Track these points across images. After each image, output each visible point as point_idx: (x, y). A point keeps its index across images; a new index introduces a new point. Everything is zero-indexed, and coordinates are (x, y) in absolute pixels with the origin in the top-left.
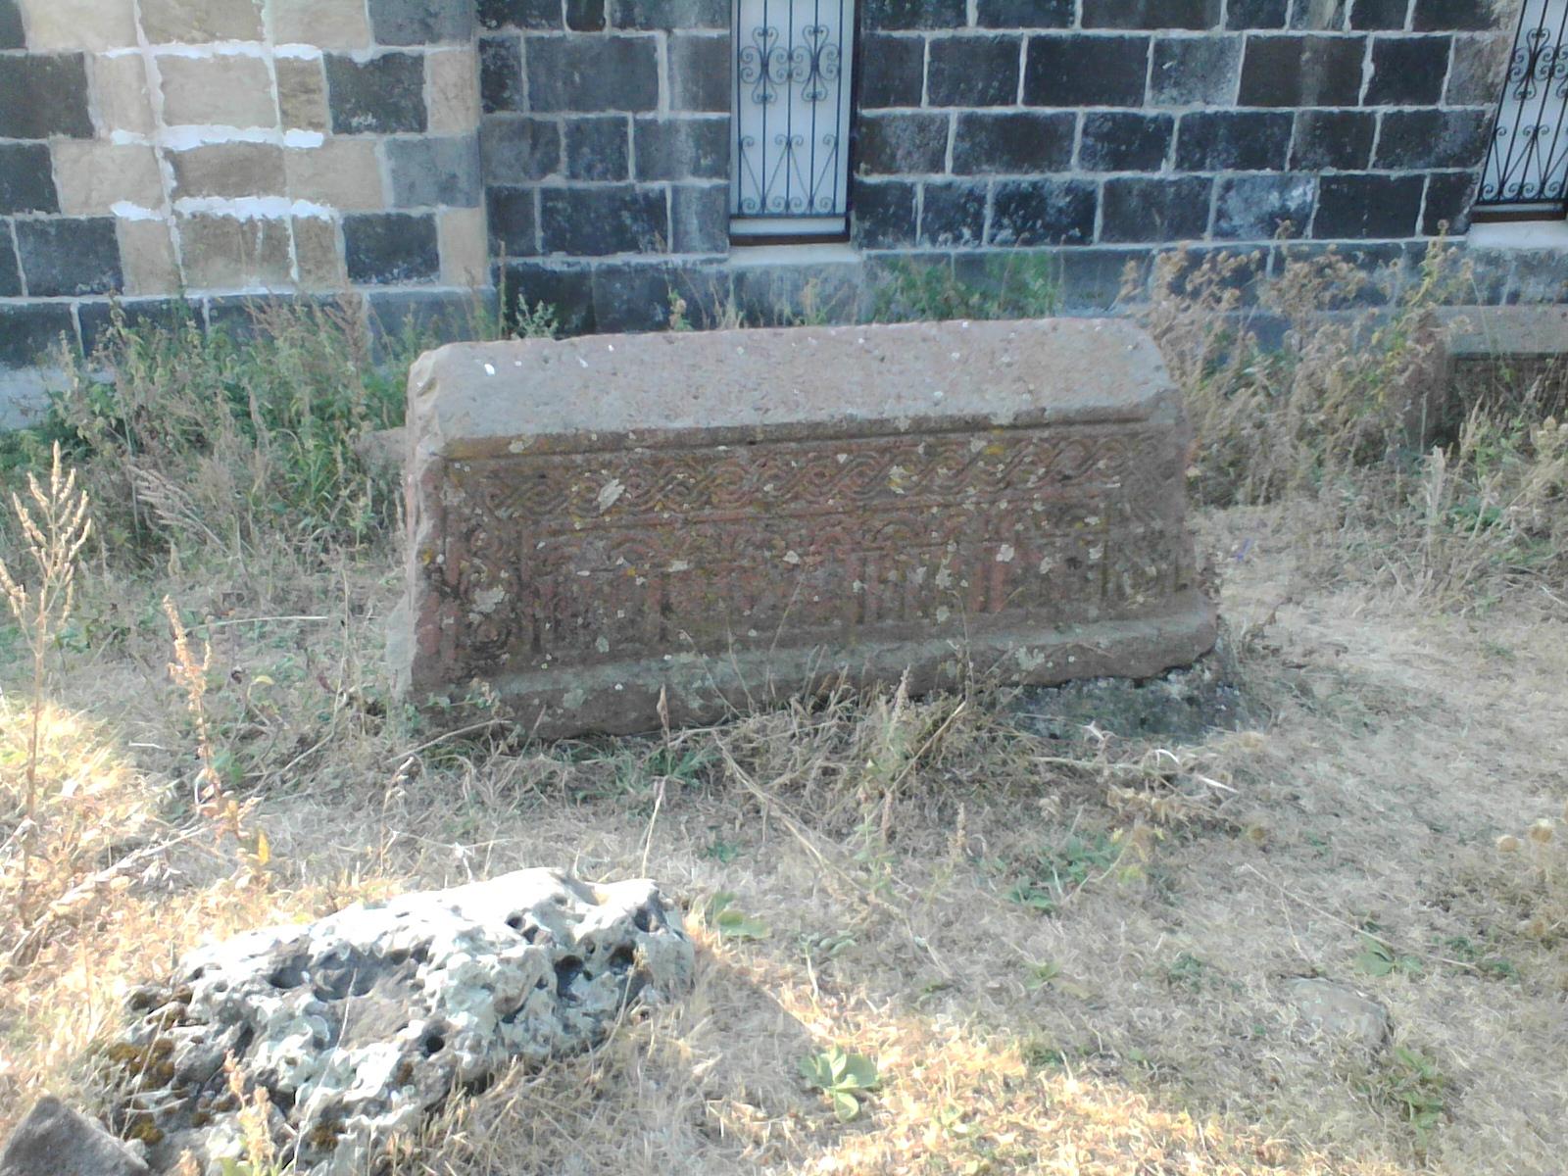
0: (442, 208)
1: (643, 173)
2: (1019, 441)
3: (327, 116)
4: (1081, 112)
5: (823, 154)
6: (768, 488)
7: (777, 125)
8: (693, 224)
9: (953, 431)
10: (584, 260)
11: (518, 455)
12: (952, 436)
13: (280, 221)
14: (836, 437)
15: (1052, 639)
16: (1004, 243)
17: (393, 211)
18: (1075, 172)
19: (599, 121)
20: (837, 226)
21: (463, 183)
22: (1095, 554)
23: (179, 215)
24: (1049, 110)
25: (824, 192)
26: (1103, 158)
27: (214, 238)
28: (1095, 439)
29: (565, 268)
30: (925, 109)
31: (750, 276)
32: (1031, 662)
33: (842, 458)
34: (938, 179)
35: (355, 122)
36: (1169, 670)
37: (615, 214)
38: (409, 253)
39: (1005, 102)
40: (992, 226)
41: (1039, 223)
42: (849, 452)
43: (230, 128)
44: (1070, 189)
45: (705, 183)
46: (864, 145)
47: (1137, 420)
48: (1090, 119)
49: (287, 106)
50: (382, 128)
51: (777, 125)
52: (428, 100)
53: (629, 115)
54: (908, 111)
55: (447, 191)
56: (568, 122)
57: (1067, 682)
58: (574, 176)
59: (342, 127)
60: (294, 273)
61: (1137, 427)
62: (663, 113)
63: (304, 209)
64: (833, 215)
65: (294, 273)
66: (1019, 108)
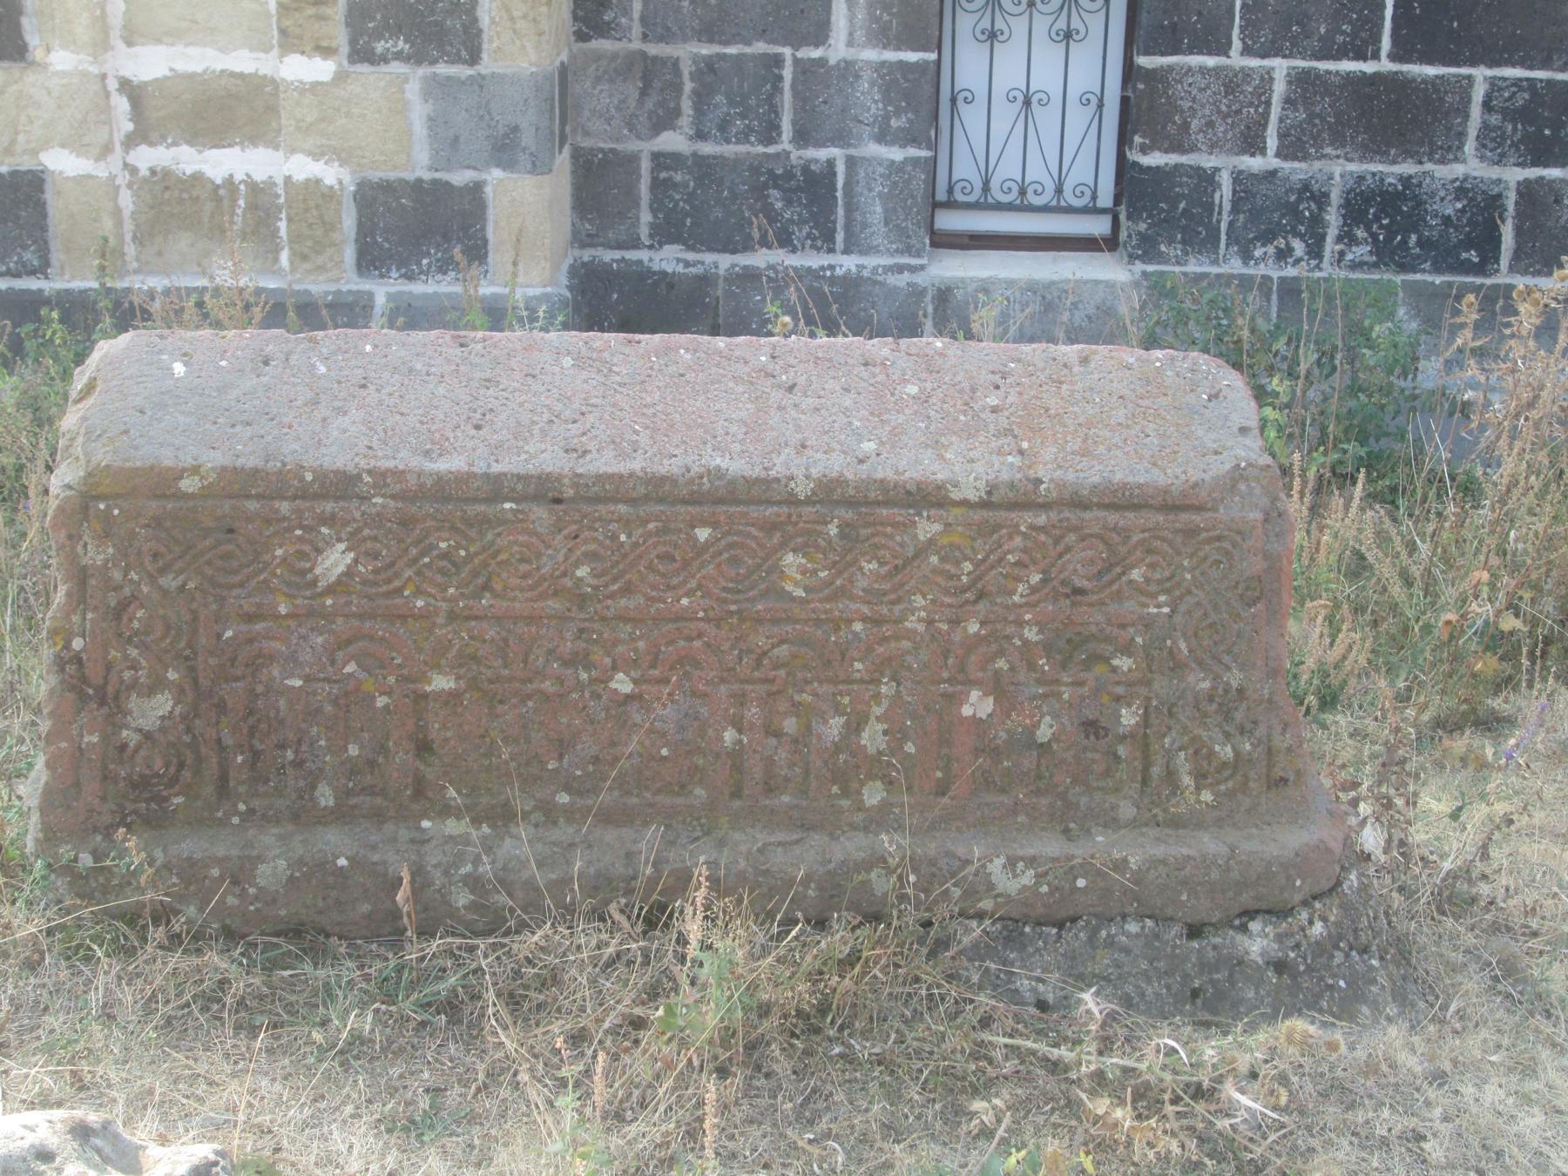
0: (497, 173)
1: (803, 136)
2: (997, 527)
3: (341, 38)
4: (1481, 73)
5: (1079, 118)
6: (582, 572)
7: (1009, 73)
8: (876, 212)
10: (709, 258)
11: (192, 496)
13: (271, 183)
14: (694, 499)
15: (1051, 846)
16: (1356, 266)
17: (427, 176)
18: (1471, 166)
19: (740, 57)
20: (1098, 227)
21: (528, 139)
22: (1129, 718)
23: (134, 171)
24: (1431, 71)
25: (1079, 174)
26: (1514, 145)
27: (176, 206)
28: (1125, 533)
29: (680, 269)
30: (1236, 59)
31: (959, 294)
32: (1010, 882)
33: (703, 534)
34: (1255, 163)
35: (380, 47)
36: (1251, 914)
37: (759, 191)
38: (446, 237)
39: (1361, 56)
40: (1339, 239)
41: (1414, 238)
42: (714, 525)
43: (211, 52)
44: (1462, 189)
45: (896, 154)
46: (1141, 109)
47: (1200, 508)
48: (1494, 85)
49: (287, 23)
50: (417, 58)
51: (1009, 73)
52: (485, 21)
53: (787, 51)
54: (1211, 61)
55: (504, 151)
56: (696, 59)
57: (1074, 920)
58: (700, 136)
59: (362, 54)
60: (284, 257)
61: (1196, 518)
62: (837, 49)
63: (302, 168)
64: (1092, 210)
65: (284, 257)
66: (1385, 65)
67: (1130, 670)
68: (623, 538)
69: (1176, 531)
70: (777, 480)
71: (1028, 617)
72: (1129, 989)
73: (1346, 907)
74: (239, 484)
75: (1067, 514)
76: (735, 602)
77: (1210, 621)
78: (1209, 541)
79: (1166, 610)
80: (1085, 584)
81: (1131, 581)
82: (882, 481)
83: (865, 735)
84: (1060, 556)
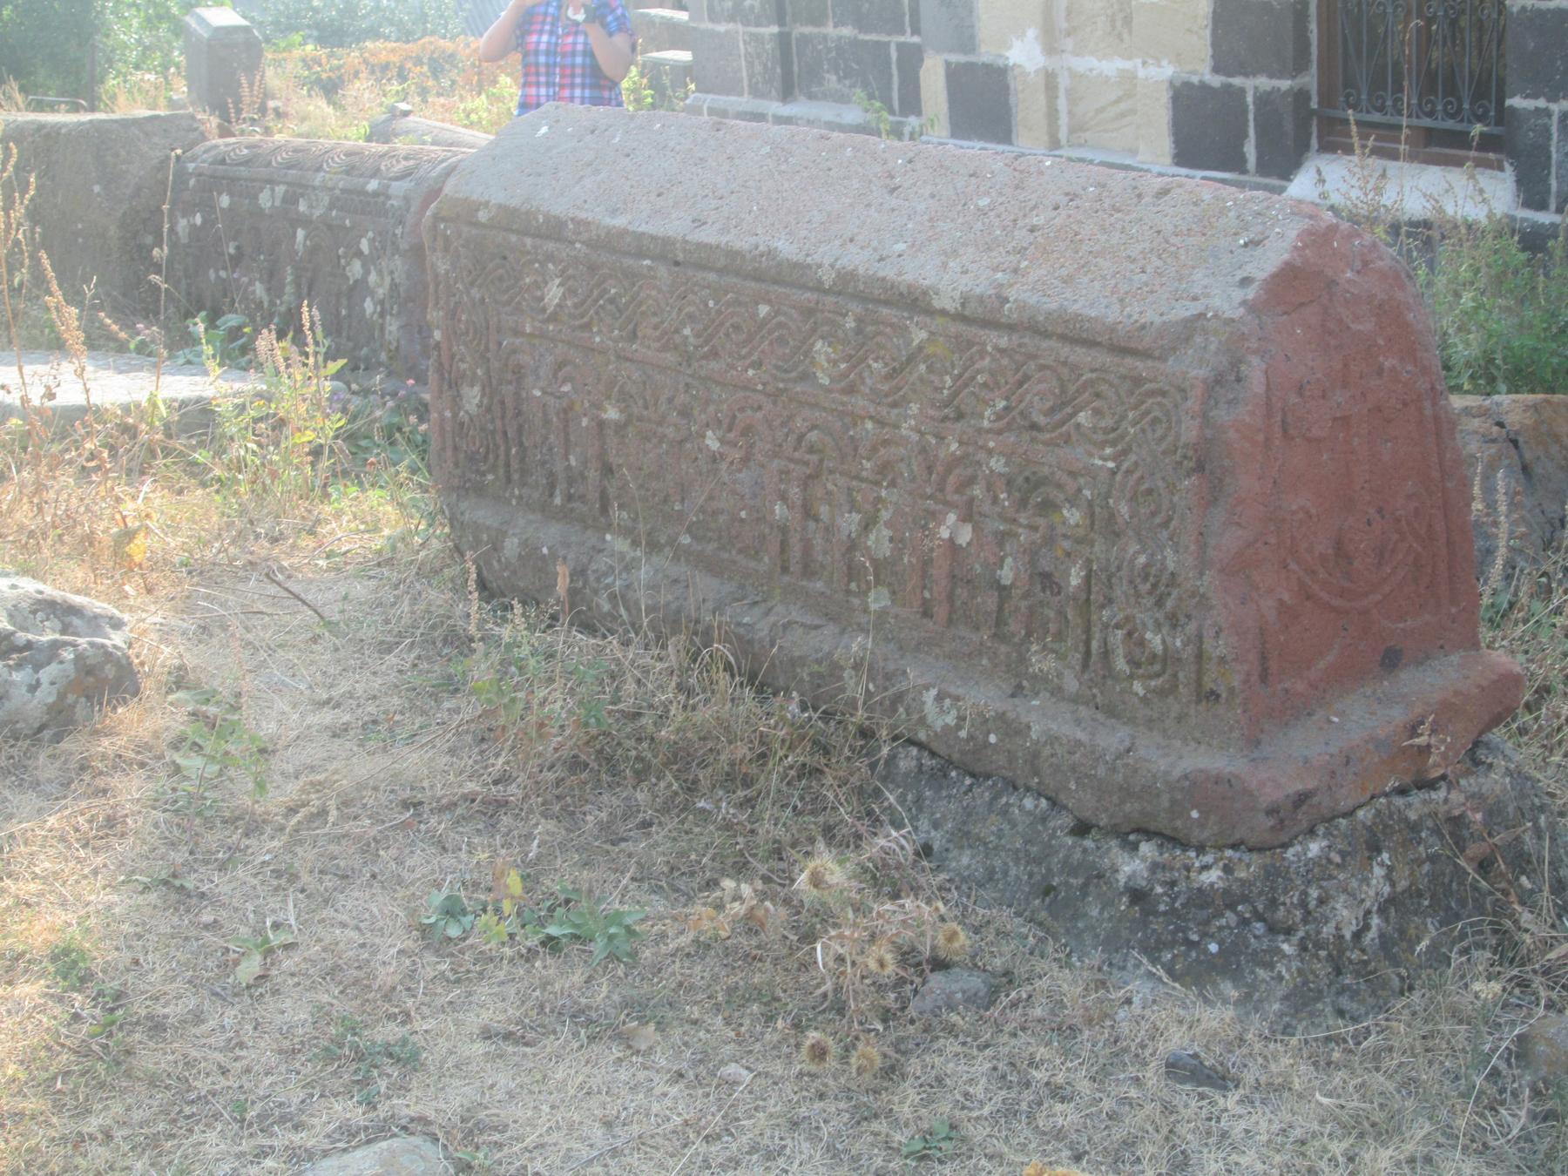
2: (970, 344)
6: (687, 331)
9: (887, 303)
11: (483, 226)
12: (885, 311)
14: (758, 277)
28: (1074, 368)
32: (938, 717)
33: (764, 310)
36: (1149, 834)
42: (769, 302)
47: (1145, 354)
57: (988, 777)
61: (1141, 366)
67: (1077, 525)
68: (711, 303)
69: (1123, 378)
70: (809, 266)
71: (991, 444)
72: (998, 863)
73: (1273, 874)
74: (513, 220)
75: (1026, 340)
76: (783, 380)
77: (1146, 486)
78: (1152, 393)
79: (1111, 465)
80: (1041, 420)
81: (1078, 426)
82: (884, 279)
83: (872, 537)
84: (1020, 384)
